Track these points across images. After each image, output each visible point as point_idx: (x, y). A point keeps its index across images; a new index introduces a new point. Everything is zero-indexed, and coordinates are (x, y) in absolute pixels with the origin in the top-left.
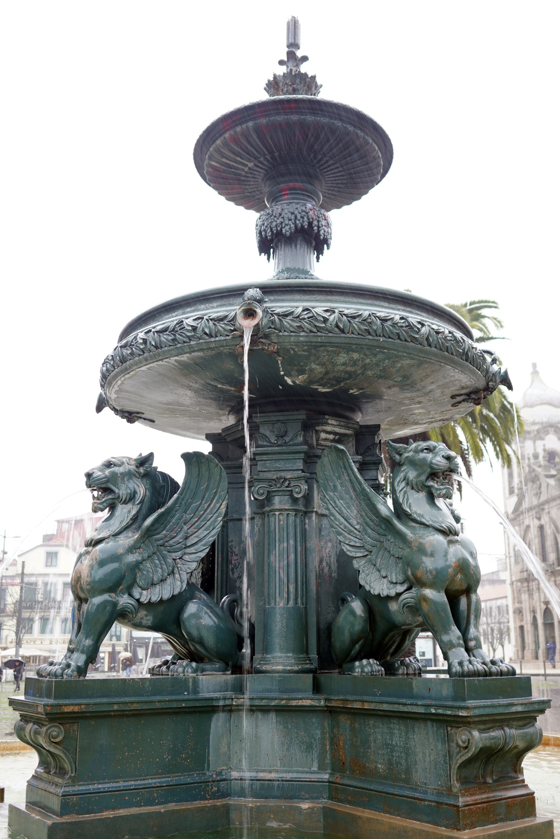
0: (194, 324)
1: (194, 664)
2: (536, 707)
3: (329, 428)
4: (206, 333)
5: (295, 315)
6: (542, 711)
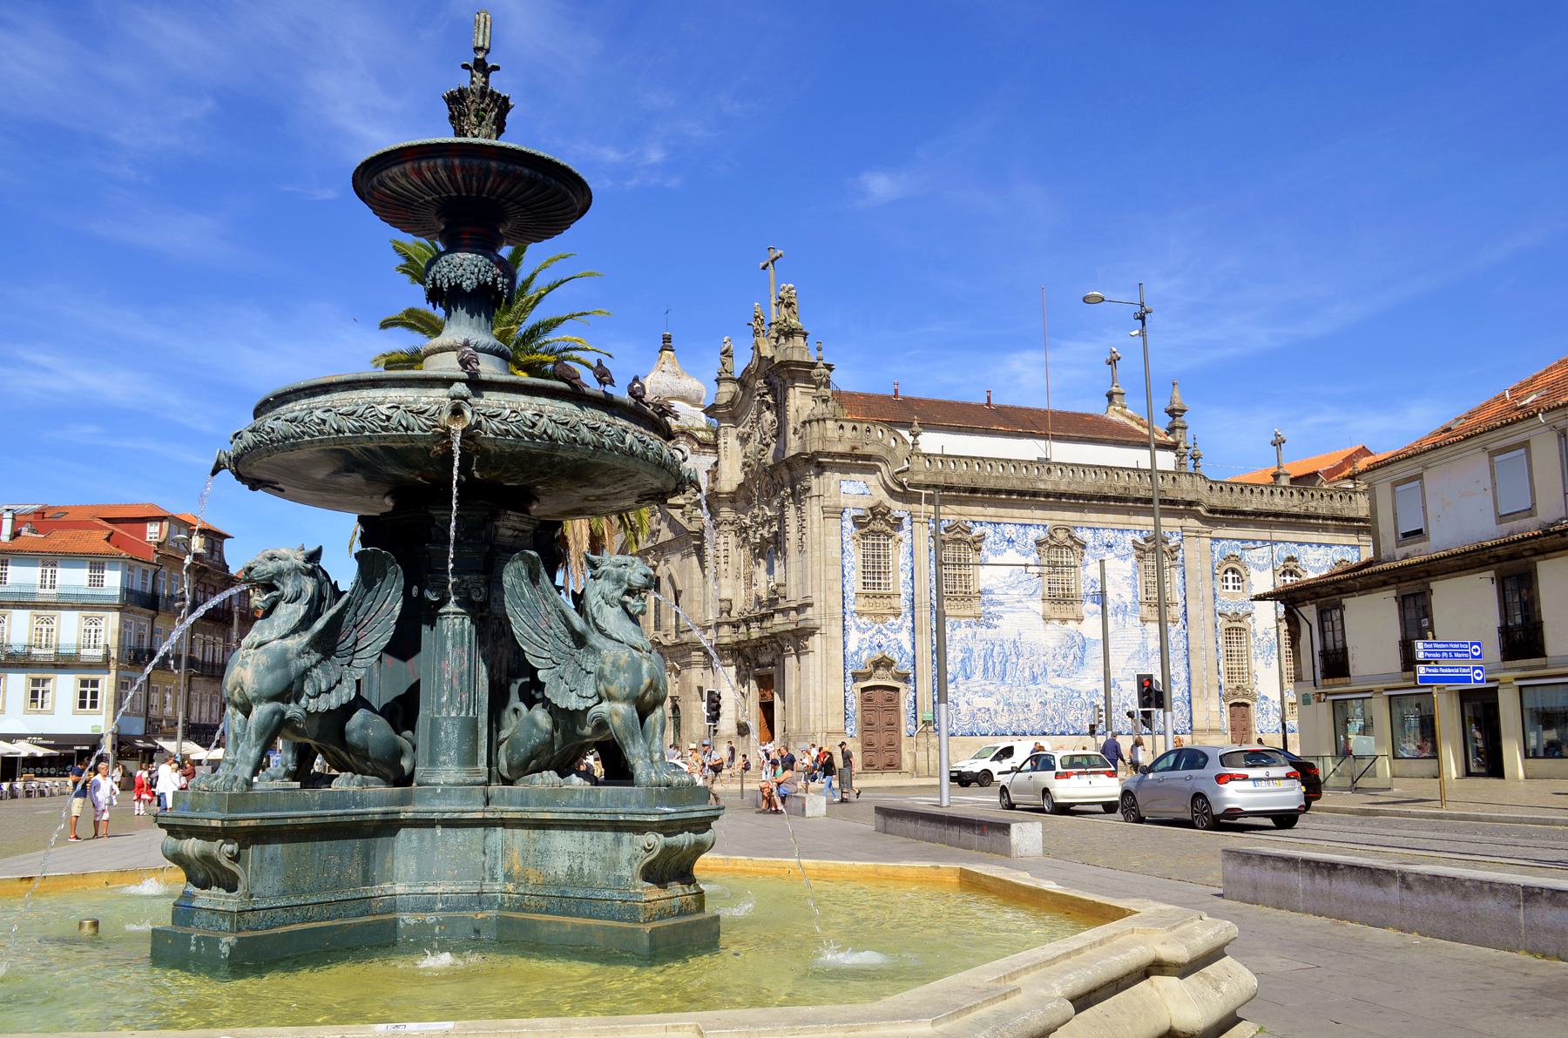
0: (388, 412)
1: (359, 776)
2: (713, 813)
3: (510, 524)
4: (402, 425)
5: (503, 417)
6: (716, 817)
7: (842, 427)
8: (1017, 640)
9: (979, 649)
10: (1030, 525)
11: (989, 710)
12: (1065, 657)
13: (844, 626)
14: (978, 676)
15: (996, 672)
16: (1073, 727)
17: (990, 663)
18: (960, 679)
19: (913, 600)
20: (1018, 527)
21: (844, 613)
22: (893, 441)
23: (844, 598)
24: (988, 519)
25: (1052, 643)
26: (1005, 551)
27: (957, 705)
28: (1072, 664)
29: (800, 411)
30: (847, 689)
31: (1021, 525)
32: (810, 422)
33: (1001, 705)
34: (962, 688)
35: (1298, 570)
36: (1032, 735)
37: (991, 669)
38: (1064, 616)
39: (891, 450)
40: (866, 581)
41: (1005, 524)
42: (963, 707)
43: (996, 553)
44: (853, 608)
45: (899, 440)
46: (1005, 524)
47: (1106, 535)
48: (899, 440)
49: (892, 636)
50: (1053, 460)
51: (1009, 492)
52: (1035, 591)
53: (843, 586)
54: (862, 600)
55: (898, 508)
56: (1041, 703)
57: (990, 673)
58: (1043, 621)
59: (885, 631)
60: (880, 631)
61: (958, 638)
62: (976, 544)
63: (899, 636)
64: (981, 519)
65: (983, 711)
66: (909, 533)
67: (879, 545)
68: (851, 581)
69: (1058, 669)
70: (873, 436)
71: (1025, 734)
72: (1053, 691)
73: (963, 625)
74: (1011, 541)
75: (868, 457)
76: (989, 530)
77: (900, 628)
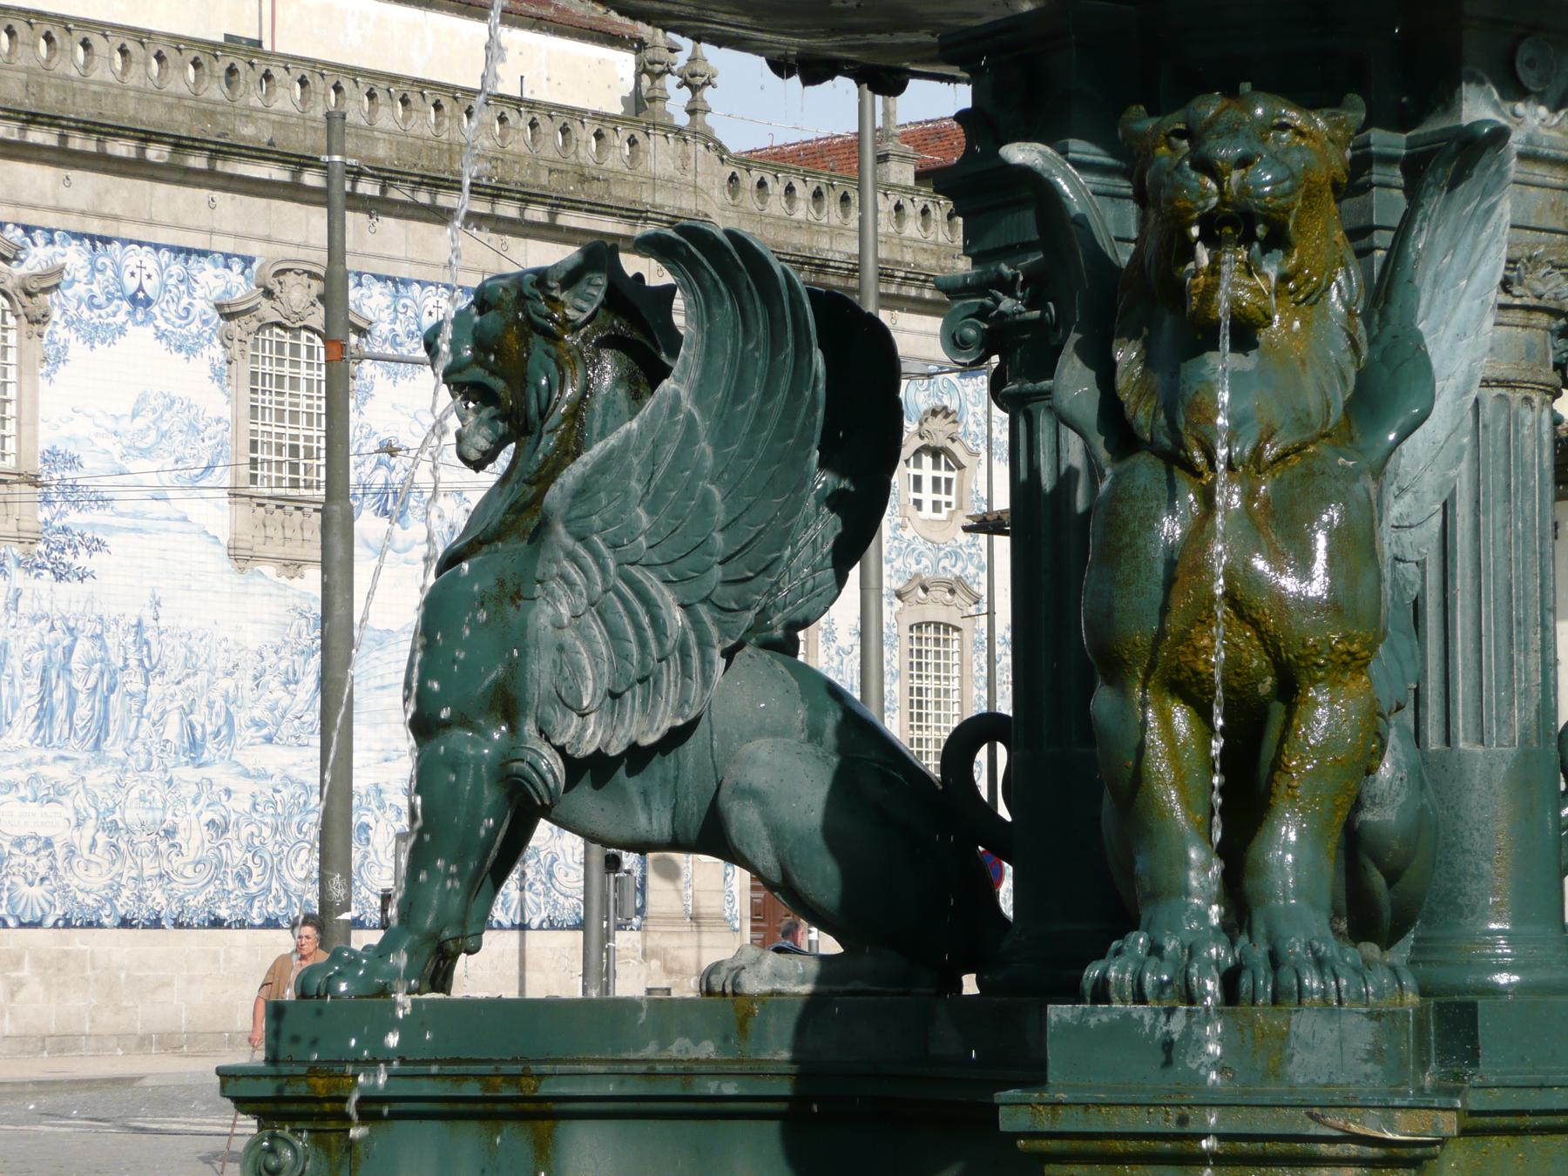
8: (148, 621)
10: (203, 254)
11: (48, 843)
12: (290, 680)
15: (79, 723)
17: (60, 693)
20: (165, 256)
24: (74, 224)
25: (254, 637)
26: (121, 330)
31: (177, 250)
33: (89, 829)
35: (956, 448)
36: (178, 925)
37: (61, 713)
41: (126, 242)
43: (95, 335)
46: (126, 242)
47: (431, 302)
52: (209, 468)
57: (60, 727)
58: (228, 565)
64: (51, 220)
65: (30, 846)
69: (267, 717)
71: (156, 924)
72: (244, 788)
74: (139, 301)
76: (74, 257)
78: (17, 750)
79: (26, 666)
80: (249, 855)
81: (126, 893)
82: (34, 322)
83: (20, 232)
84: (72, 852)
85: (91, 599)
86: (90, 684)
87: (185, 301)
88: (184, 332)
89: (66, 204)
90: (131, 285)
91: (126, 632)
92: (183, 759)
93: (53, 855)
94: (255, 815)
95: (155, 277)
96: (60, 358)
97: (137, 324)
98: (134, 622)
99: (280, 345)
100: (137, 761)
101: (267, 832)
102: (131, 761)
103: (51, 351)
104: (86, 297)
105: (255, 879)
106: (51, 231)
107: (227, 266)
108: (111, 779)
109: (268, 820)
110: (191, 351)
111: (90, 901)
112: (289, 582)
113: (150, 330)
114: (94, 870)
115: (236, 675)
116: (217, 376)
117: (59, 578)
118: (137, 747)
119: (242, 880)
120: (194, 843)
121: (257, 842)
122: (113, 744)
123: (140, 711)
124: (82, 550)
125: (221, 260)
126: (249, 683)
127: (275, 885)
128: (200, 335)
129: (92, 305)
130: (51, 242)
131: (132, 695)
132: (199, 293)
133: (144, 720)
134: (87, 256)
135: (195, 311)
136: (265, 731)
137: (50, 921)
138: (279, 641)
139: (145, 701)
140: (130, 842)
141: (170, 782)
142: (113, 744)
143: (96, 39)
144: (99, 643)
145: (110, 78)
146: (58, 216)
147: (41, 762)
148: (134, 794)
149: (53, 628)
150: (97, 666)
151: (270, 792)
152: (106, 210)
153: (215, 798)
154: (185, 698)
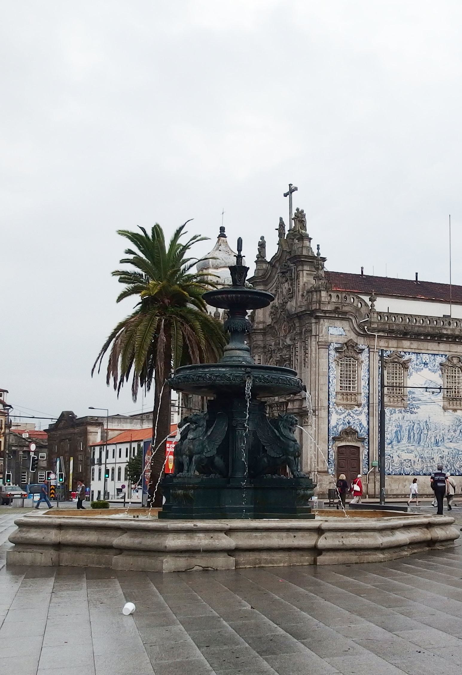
7: (330, 295)
8: (428, 421)
9: (405, 426)
10: (437, 355)
11: (410, 460)
12: (455, 431)
13: (329, 411)
14: (405, 441)
16: (458, 471)
17: (412, 434)
18: (395, 443)
19: (369, 397)
20: (430, 355)
21: (329, 403)
22: (360, 305)
23: (329, 394)
24: (413, 351)
25: (448, 423)
26: (422, 369)
27: (392, 457)
28: (459, 435)
29: (306, 285)
30: (330, 447)
31: (432, 354)
32: (312, 292)
34: (395, 448)
37: (412, 437)
38: (455, 407)
39: (358, 310)
40: (342, 385)
42: (396, 459)
43: (417, 370)
44: (334, 400)
45: (363, 304)
48: (363, 304)
49: (356, 417)
50: (452, 317)
51: (426, 335)
53: (329, 388)
54: (340, 397)
55: (362, 343)
56: (440, 457)
58: (443, 410)
59: (352, 415)
60: (349, 414)
61: (393, 419)
62: (405, 366)
63: (360, 417)
64: (409, 350)
66: (367, 358)
67: (350, 365)
68: (333, 385)
69: (450, 438)
70: (348, 301)
72: (447, 451)
73: (397, 412)
74: (426, 364)
75: (346, 313)
76: (413, 357)
77: (361, 413)
78: (404, 444)
79: (405, 429)
80: (448, 463)
81: (424, 469)
82: (406, 368)
83: (404, 353)
84: (414, 462)
85: (417, 417)
86: (417, 432)
87: (434, 363)
88: (434, 369)
89: (412, 347)
90: (424, 361)
91: (424, 423)
92: (435, 445)
93: (411, 462)
94: (449, 456)
95: (428, 359)
96: (411, 374)
97: (425, 368)
98: (425, 421)
99: (452, 371)
100: (426, 446)
101: (451, 458)
102: (425, 446)
103: (410, 373)
104: (416, 364)
105: (449, 467)
106: (409, 352)
107: (442, 357)
108: (422, 449)
109: (451, 456)
110: (435, 372)
111: (418, 471)
112: (454, 413)
113: (427, 369)
114: (419, 465)
115: (445, 430)
116: (440, 376)
117: (411, 413)
118: (426, 443)
119: (447, 468)
120: (437, 460)
121: (449, 460)
122: (422, 442)
123: (427, 437)
124: (416, 409)
125: (441, 356)
126: (447, 431)
127: (453, 468)
128: (437, 369)
129: (417, 365)
130: (409, 354)
131: (425, 434)
132: (437, 362)
133: (427, 439)
134: (416, 357)
135: (436, 365)
136: (450, 440)
137: (411, 474)
138: (452, 424)
139: (427, 435)
140: (425, 460)
141: (433, 449)
142: (422, 442)
143: (417, 318)
144: (419, 425)
145: (420, 325)
146: (411, 350)
147: (409, 446)
148: (426, 452)
149: (410, 422)
150: (419, 429)
151: (451, 451)
152: (419, 348)
153: (441, 452)
154: (435, 434)
